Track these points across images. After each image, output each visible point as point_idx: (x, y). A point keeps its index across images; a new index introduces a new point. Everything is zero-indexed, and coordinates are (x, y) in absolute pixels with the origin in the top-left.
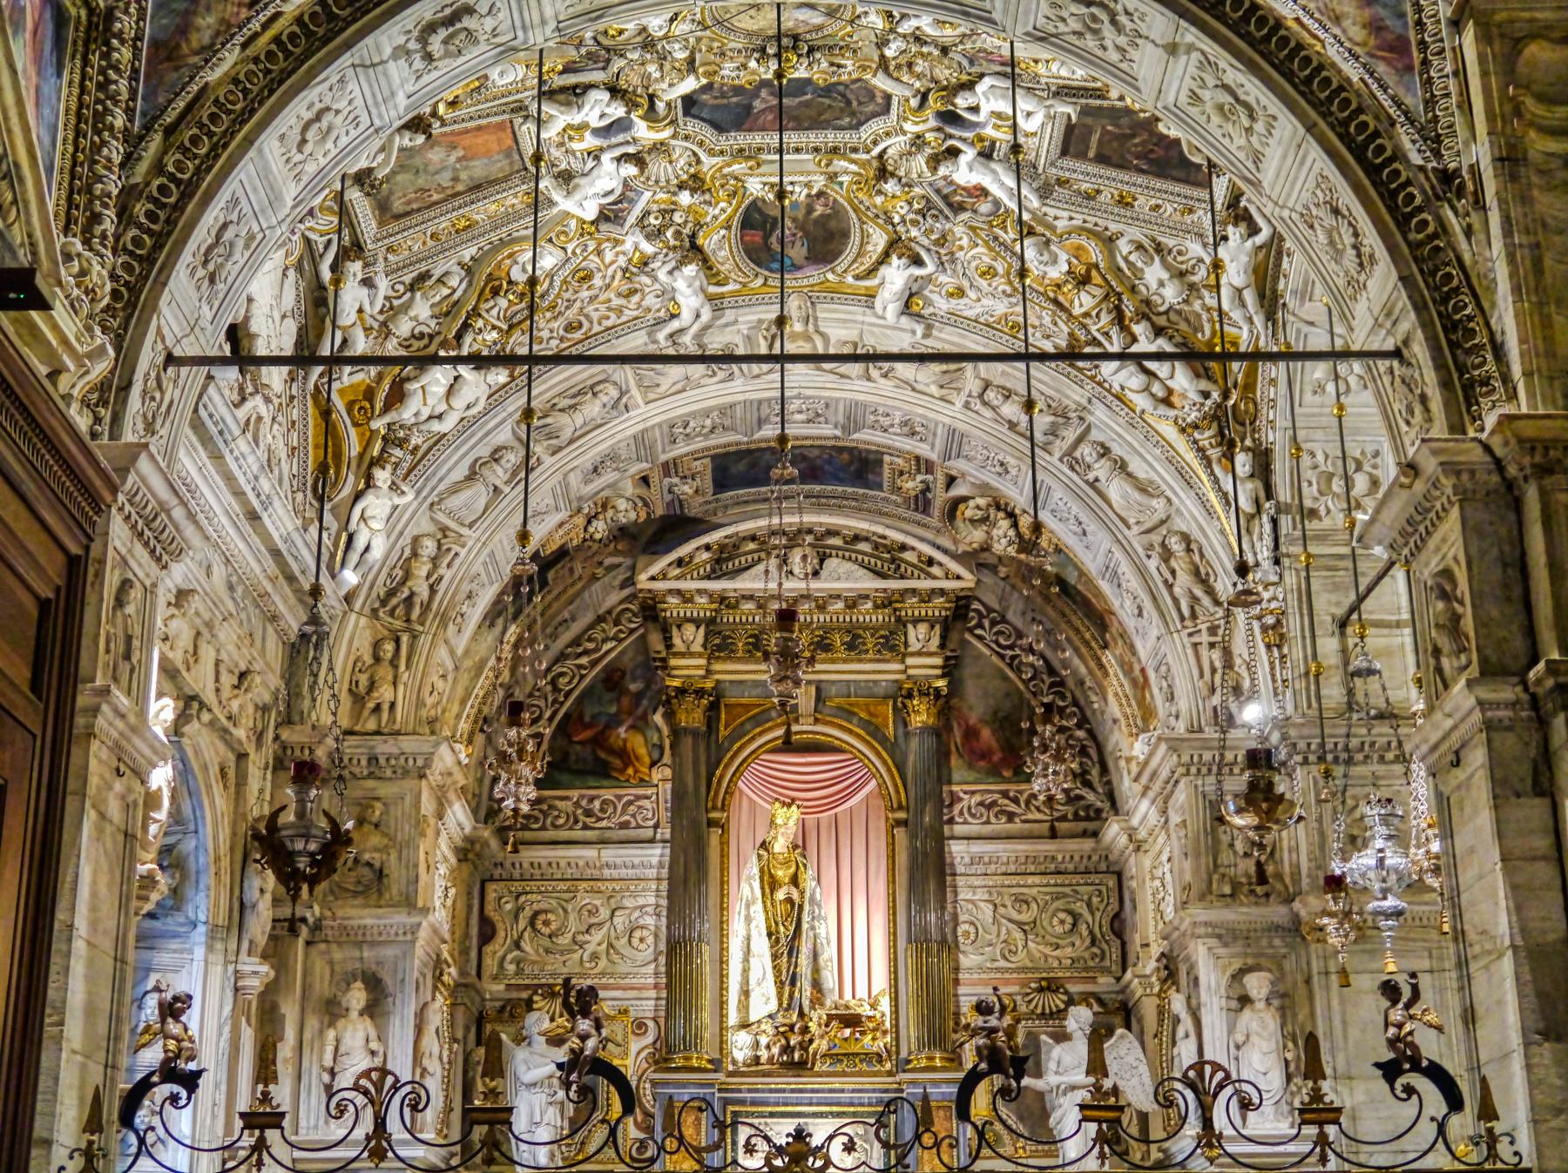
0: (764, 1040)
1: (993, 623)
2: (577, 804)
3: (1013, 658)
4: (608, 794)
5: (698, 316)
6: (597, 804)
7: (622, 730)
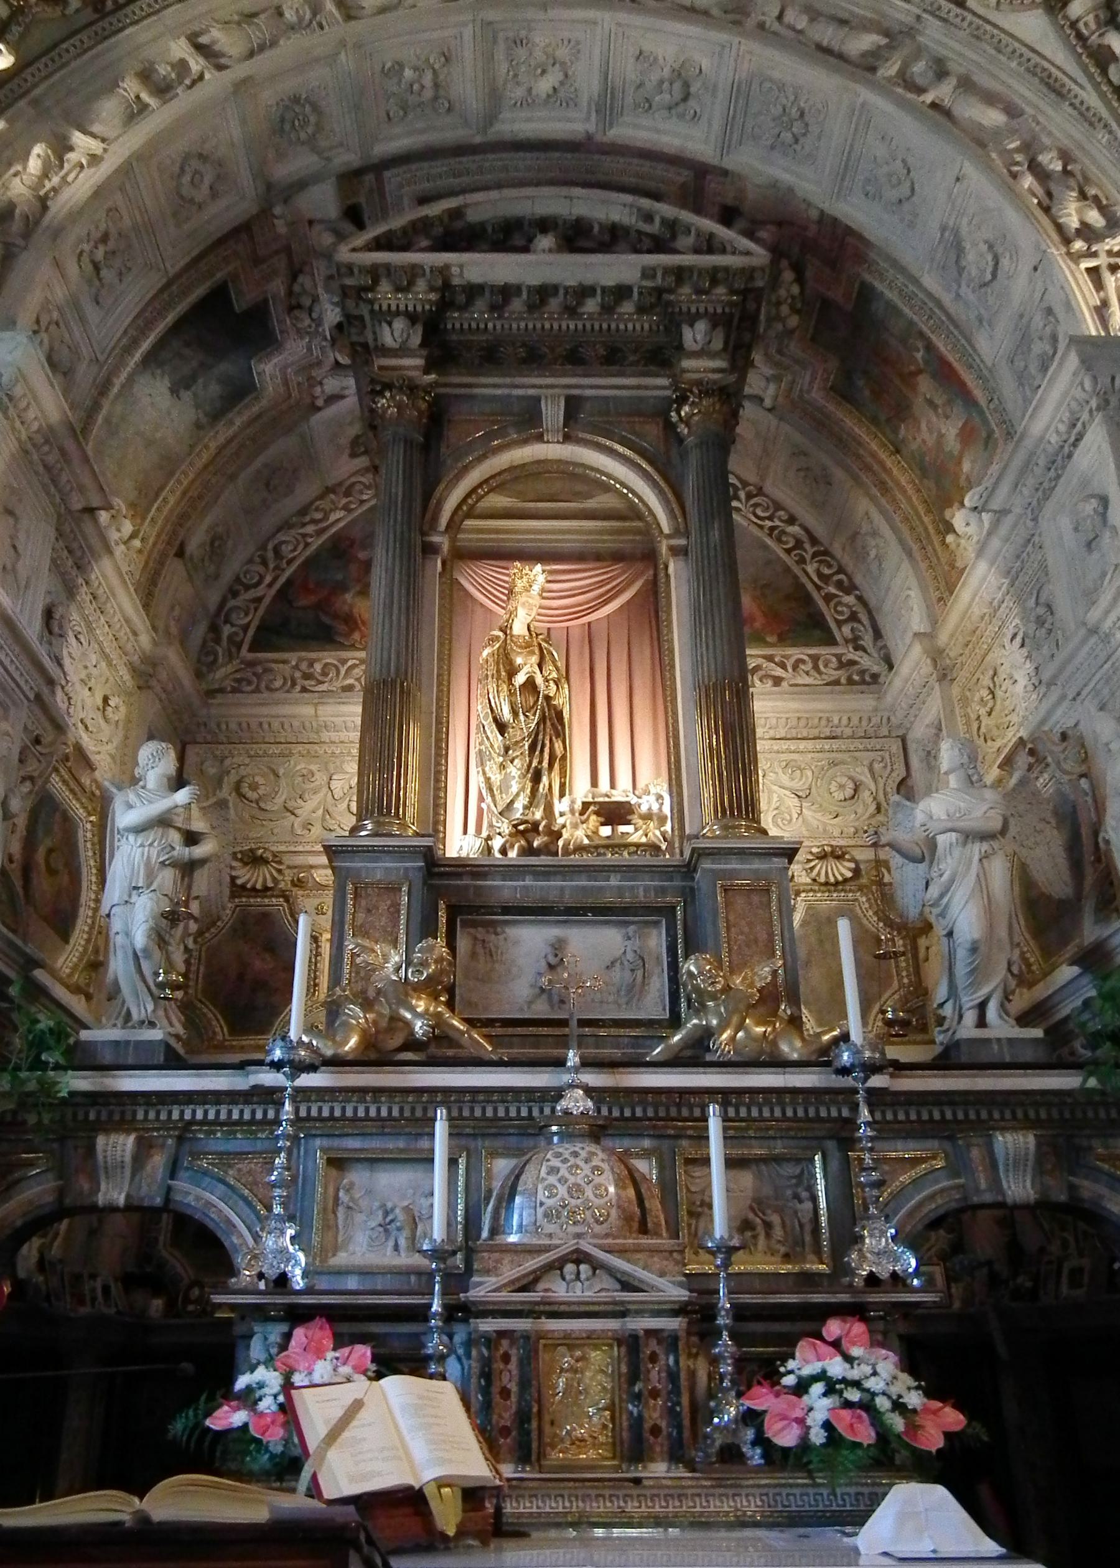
0: (497, 843)
1: (749, 496)
2: (296, 667)
3: (772, 529)
4: (329, 657)
6: (318, 667)
7: (348, 597)
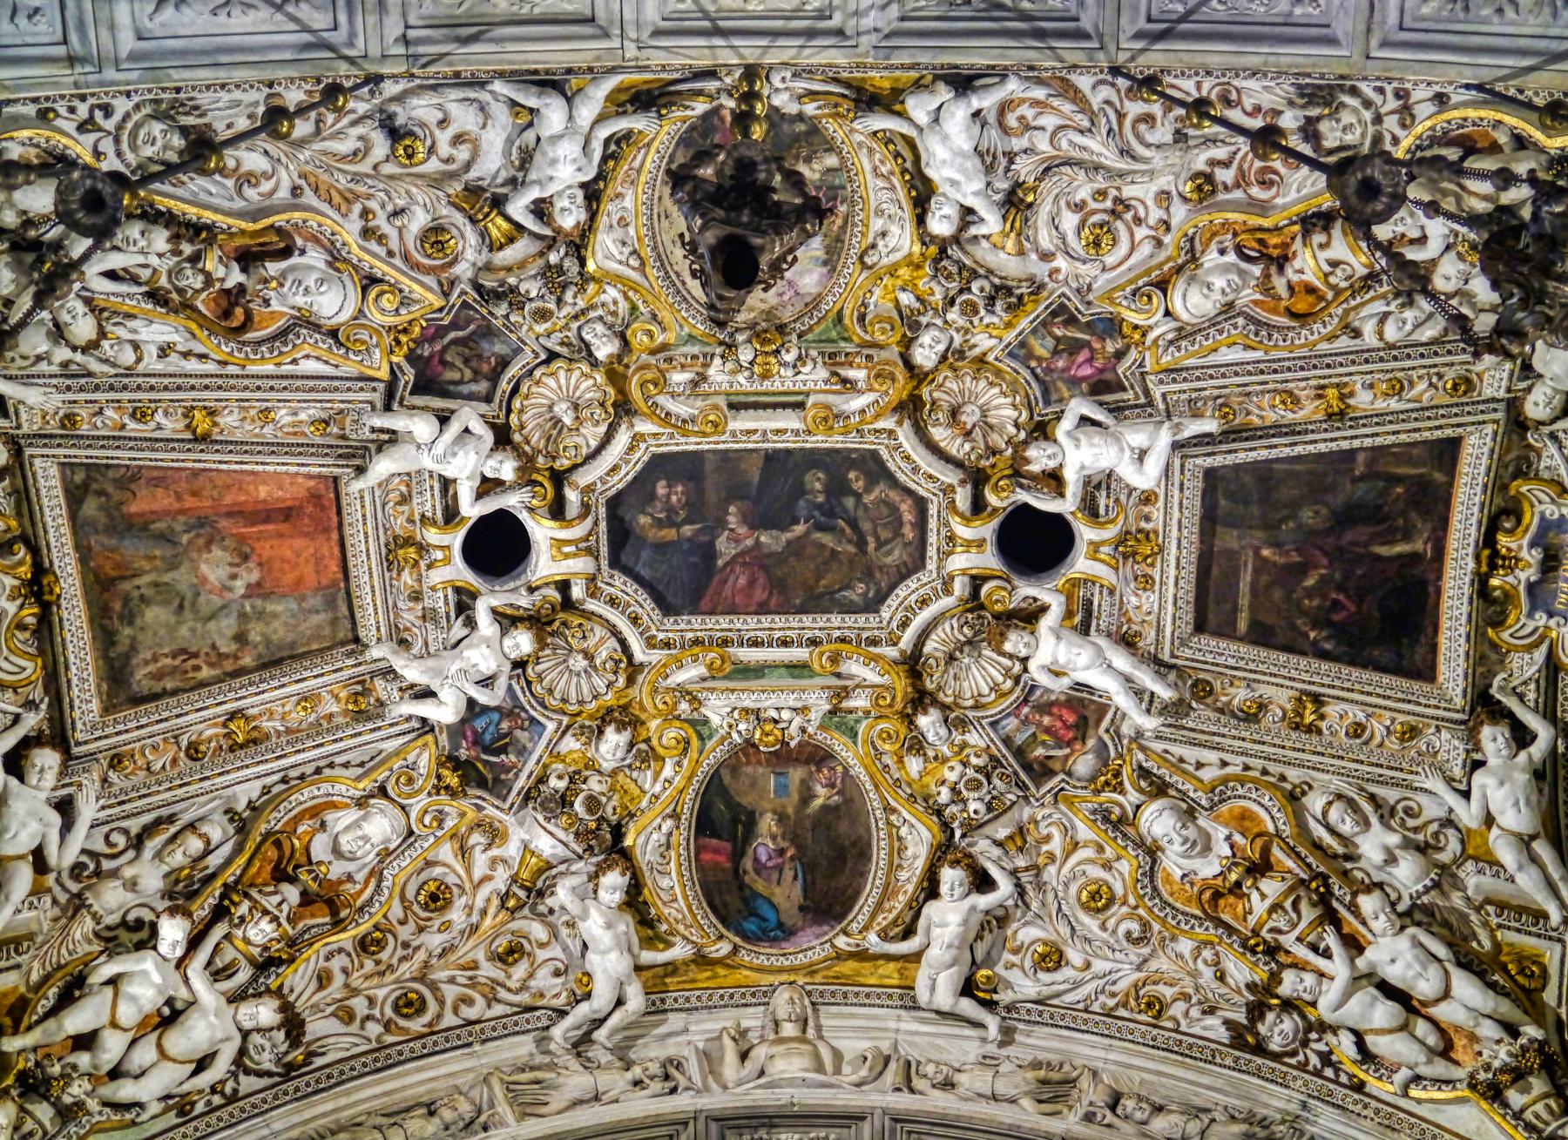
5: (620, 1002)
